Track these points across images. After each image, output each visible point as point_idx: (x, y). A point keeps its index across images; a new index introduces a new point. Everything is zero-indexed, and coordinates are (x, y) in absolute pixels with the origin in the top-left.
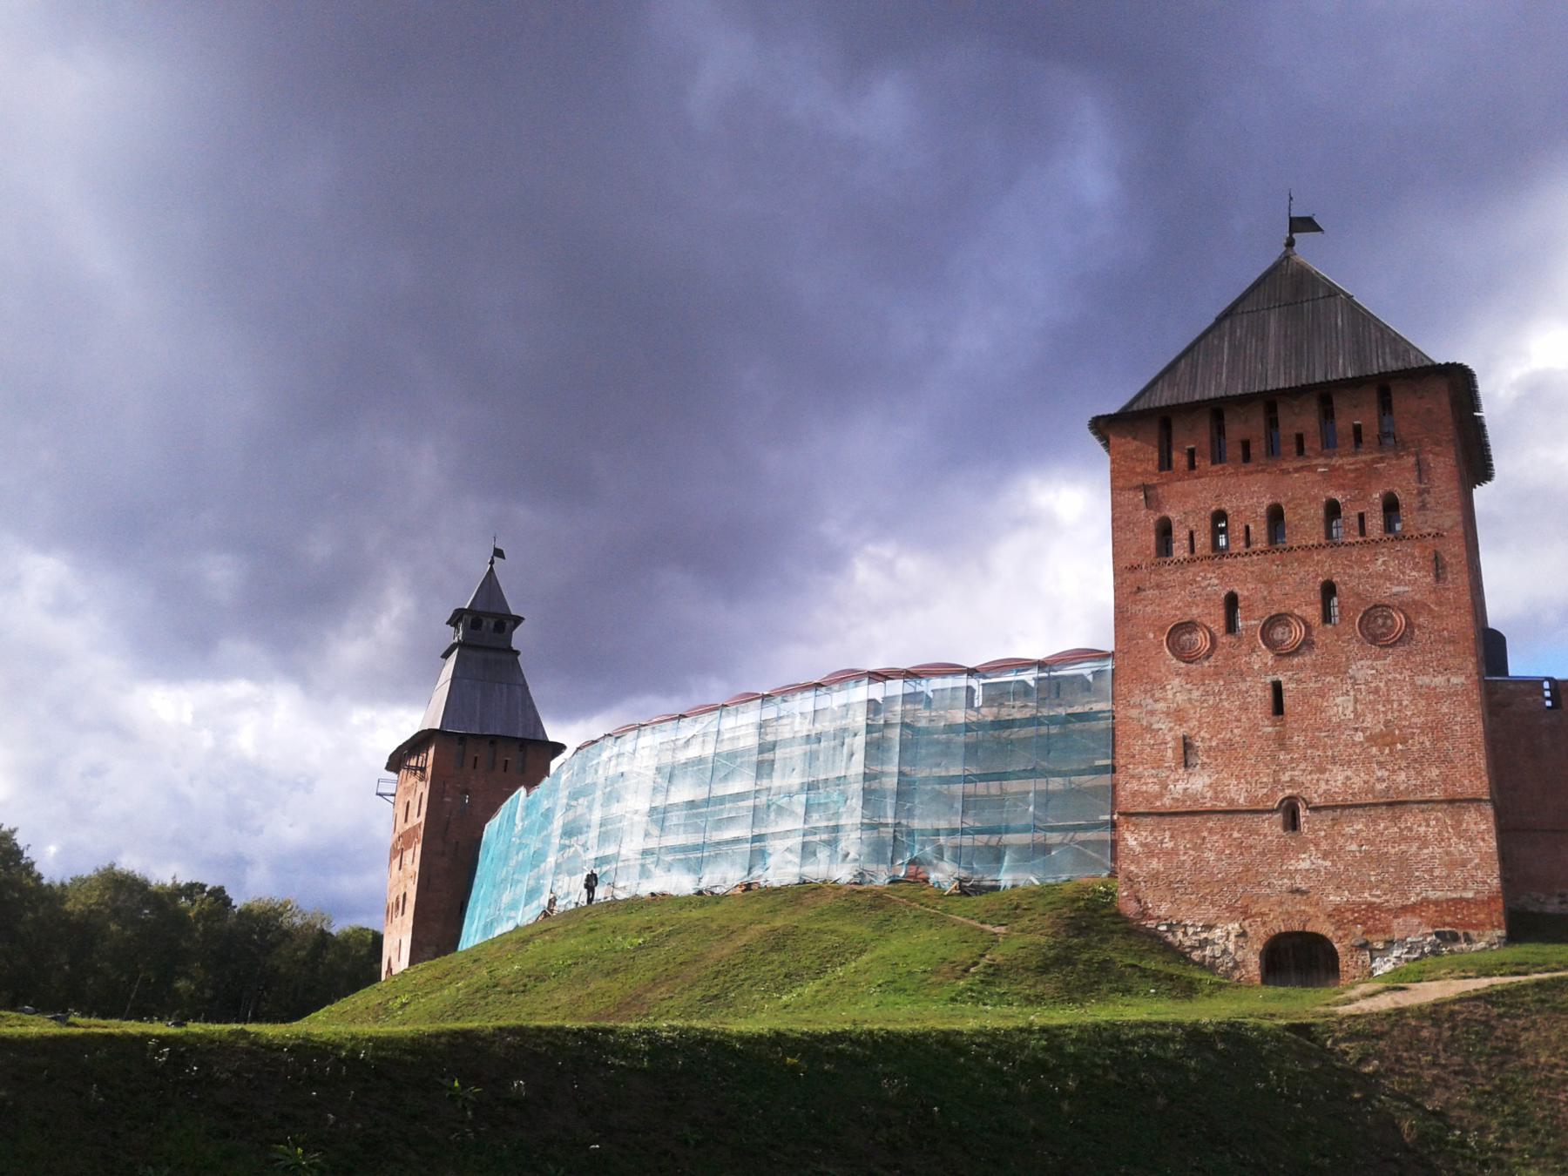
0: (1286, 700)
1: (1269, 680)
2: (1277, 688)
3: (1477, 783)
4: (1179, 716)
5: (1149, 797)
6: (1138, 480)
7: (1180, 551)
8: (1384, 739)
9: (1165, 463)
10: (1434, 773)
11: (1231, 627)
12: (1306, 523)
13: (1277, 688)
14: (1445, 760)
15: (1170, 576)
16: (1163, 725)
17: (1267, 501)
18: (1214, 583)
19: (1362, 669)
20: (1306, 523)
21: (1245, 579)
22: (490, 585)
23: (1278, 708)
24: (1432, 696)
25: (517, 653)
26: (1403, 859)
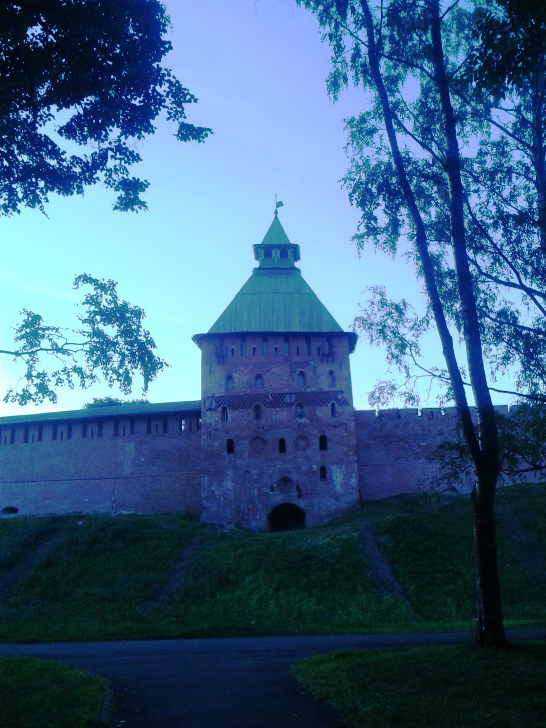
22: (276, 227)
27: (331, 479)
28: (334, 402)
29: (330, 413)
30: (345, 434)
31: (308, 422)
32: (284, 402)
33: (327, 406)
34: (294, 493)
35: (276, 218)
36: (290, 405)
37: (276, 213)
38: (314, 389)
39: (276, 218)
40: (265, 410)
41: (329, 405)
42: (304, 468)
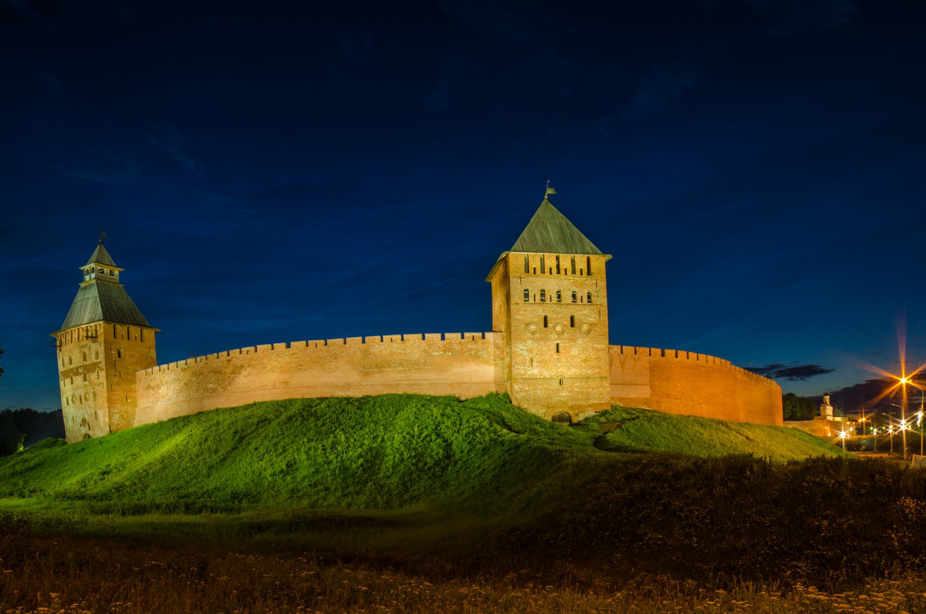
0: (560, 348)
1: (557, 342)
2: (558, 345)
3: (605, 374)
4: (530, 351)
5: (521, 375)
6: (518, 275)
7: (531, 300)
8: (585, 361)
9: (527, 271)
10: (596, 371)
11: (546, 325)
12: (567, 297)
13: (558, 345)
14: (599, 367)
15: (529, 308)
16: (525, 353)
17: (556, 289)
18: (541, 311)
19: (580, 341)
20: (567, 297)
21: (549, 310)
23: (558, 351)
24: (597, 350)
26: (588, 393)
36: (81, 374)
40: (74, 378)
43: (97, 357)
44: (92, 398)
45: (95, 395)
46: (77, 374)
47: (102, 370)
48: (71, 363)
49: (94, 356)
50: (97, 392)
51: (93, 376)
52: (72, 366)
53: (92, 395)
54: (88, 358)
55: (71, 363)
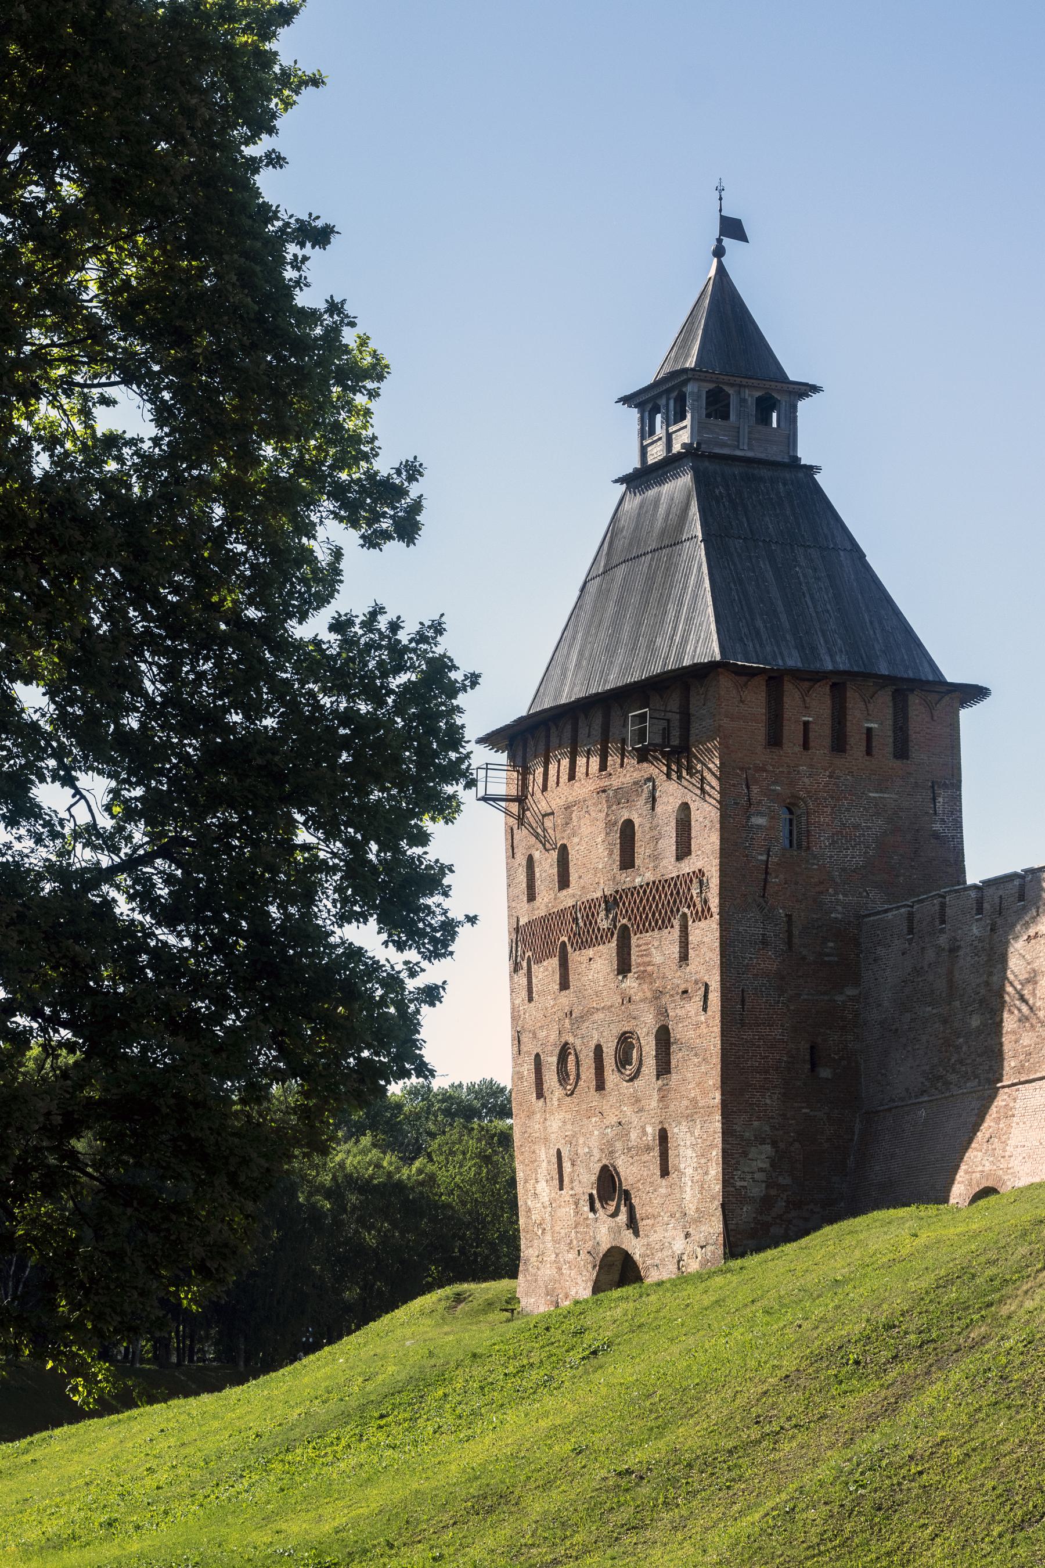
25: (811, 470)
27: (677, 1170)
28: (686, 910)
29: (676, 949)
30: (703, 1018)
31: (635, 985)
32: (599, 929)
33: (672, 927)
34: (623, 1217)
35: (721, 270)
37: (719, 252)
38: (649, 876)
39: (721, 270)
40: (576, 957)
41: (676, 923)
42: (633, 1135)
43: (684, 850)
44: (650, 1065)
45: (664, 1038)
46: (586, 938)
47: (703, 914)
48: (564, 882)
49: (669, 844)
50: (677, 1031)
51: (657, 948)
52: (567, 899)
53: (649, 1047)
54: (642, 851)
55: (564, 882)
